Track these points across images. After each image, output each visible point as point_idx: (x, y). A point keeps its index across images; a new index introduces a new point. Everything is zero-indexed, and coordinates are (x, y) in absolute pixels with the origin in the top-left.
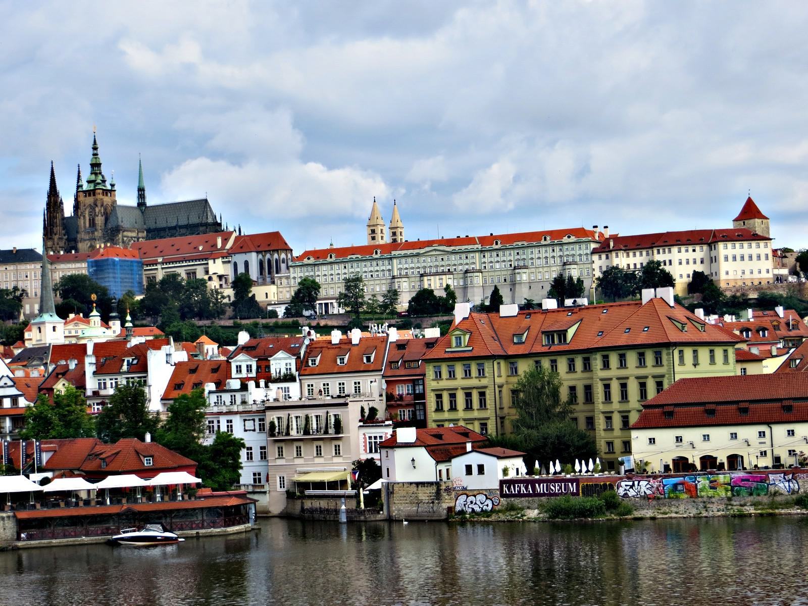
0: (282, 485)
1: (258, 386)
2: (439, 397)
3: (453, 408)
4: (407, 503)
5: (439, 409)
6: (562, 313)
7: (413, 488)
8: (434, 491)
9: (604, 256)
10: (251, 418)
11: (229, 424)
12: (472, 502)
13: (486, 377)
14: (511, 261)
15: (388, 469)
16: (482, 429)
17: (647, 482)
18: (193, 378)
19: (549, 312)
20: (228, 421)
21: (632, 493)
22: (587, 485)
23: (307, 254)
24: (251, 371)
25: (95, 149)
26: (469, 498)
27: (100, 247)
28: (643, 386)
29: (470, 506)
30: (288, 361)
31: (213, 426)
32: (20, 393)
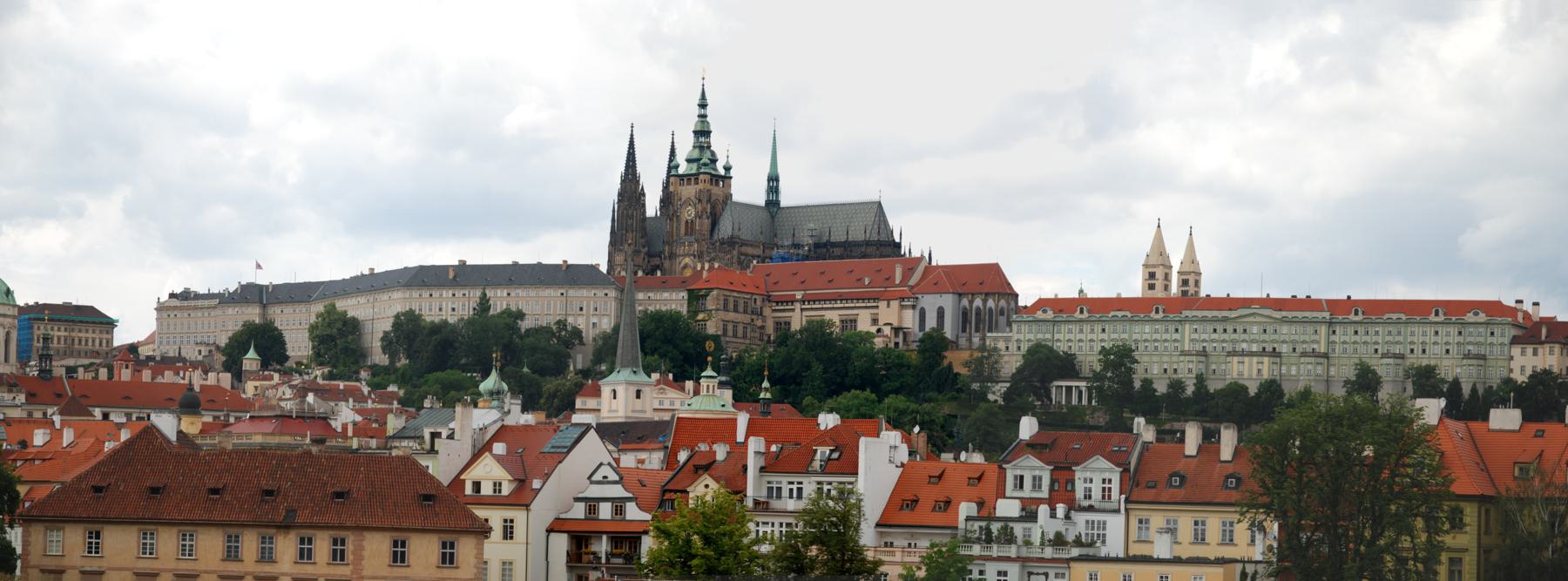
1: (1053, 515)
10: (1041, 571)
20: (999, 573)
23: (1042, 304)
24: (1040, 487)
25: (703, 106)
27: (703, 268)
32: (631, 495)
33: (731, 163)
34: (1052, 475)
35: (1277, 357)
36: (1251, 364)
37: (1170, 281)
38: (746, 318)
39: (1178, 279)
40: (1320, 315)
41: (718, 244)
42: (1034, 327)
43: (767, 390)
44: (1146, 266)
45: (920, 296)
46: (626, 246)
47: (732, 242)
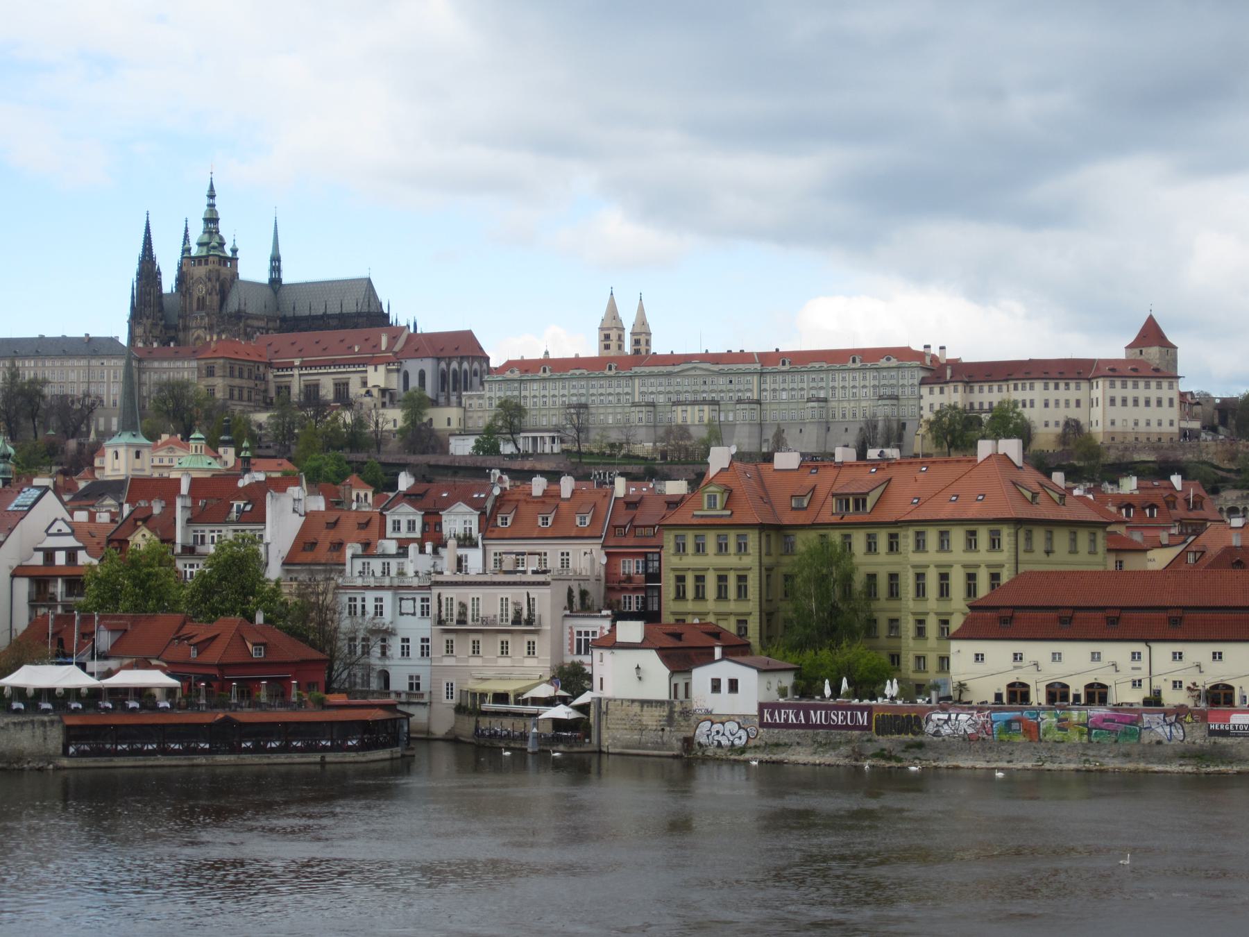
0: (450, 694)
1: (422, 550)
2: (681, 579)
3: (700, 596)
4: (626, 729)
5: (680, 595)
6: (862, 469)
7: (636, 708)
8: (664, 714)
9: (937, 389)
10: (410, 596)
11: (379, 604)
12: (718, 732)
13: (749, 554)
14: (802, 389)
15: (602, 679)
16: (739, 629)
17: (969, 716)
18: (333, 536)
19: (844, 466)
20: (376, 600)
21: (946, 730)
22: (883, 715)
23: (510, 365)
24: (414, 529)
25: (212, 196)
26: (715, 726)
27: (212, 339)
28: (971, 577)
29: (716, 738)
30: (468, 518)
31: (355, 606)
32: (81, 545)
33: (238, 246)
34: (423, 519)
35: (715, 404)
36: (693, 414)
37: (624, 342)
38: (251, 383)
39: (631, 339)
40: (752, 367)
41: (226, 317)
42: (503, 386)
43: (246, 449)
44: (601, 329)
45: (403, 361)
46: (145, 320)
47: (239, 316)
